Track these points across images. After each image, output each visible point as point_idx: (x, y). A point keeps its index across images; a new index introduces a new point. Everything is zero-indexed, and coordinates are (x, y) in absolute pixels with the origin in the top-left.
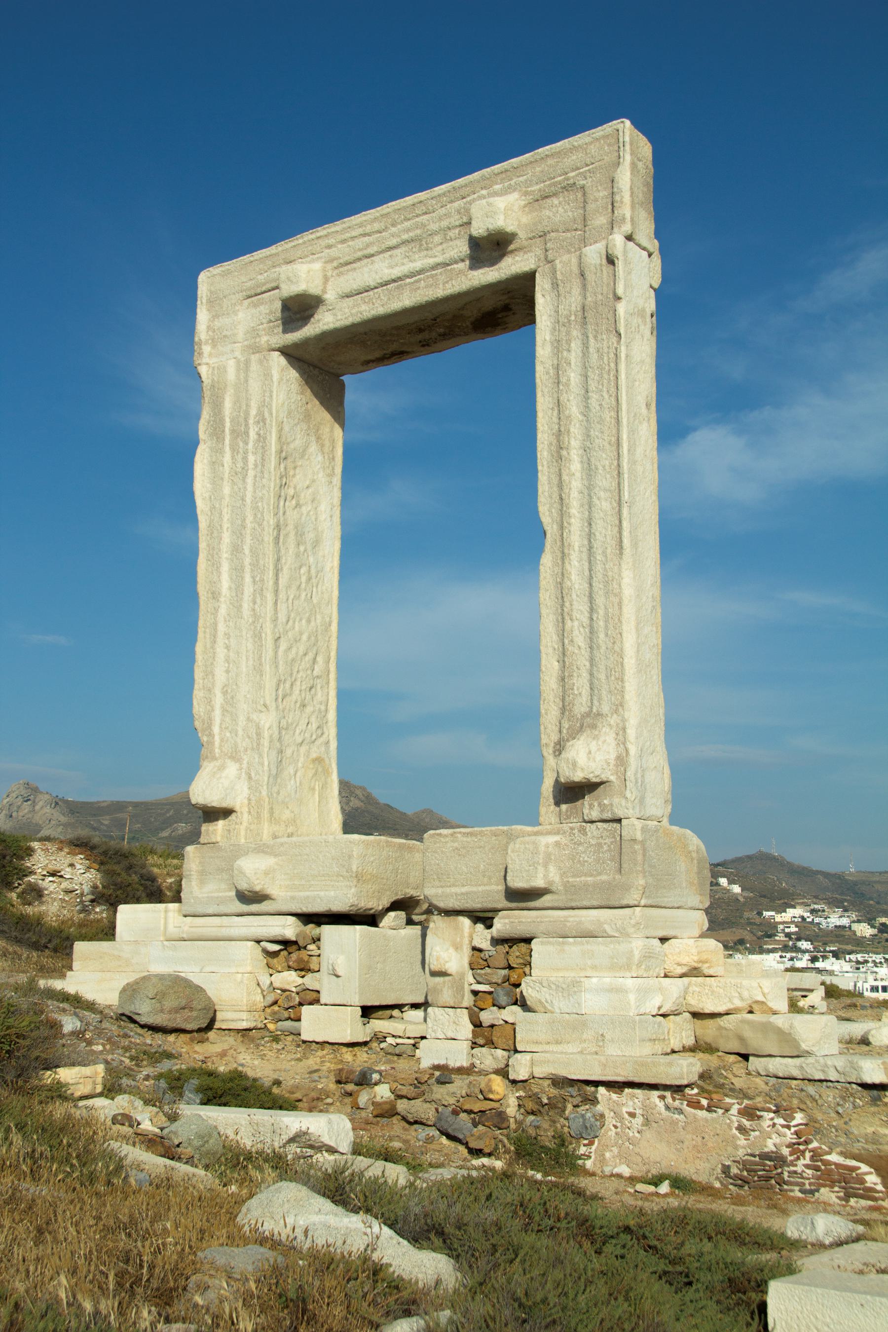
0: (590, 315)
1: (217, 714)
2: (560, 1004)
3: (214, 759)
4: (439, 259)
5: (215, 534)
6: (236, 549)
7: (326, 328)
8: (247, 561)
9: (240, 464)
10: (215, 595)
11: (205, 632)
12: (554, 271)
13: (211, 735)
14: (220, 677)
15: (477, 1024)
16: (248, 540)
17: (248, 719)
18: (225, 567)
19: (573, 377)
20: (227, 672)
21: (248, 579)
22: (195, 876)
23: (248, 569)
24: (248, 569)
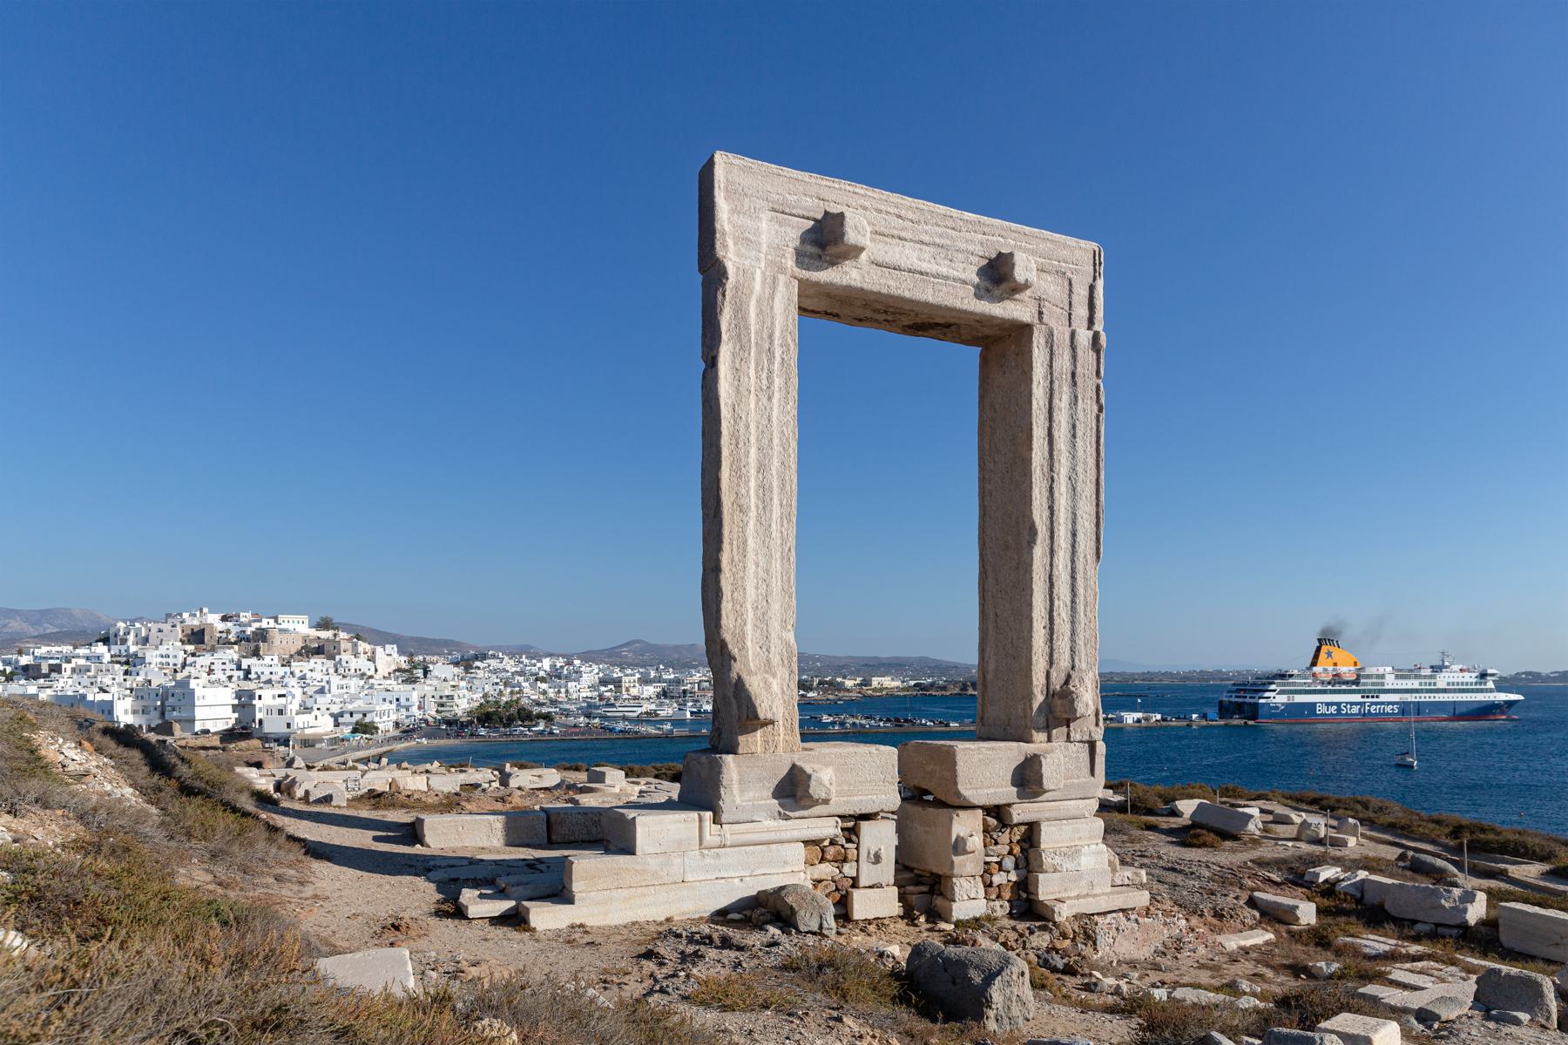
0: (1079, 380)
1: (749, 628)
2: (1068, 865)
3: (750, 673)
4: (963, 276)
5: (741, 445)
6: (762, 468)
7: (853, 283)
8: (775, 484)
9: (765, 382)
10: (743, 510)
11: (731, 544)
12: (1051, 334)
13: (743, 648)
14: (751, 592)
15: (988, 885)
16: (776, 462)
17: (780, 638)
18: (752, 484)
19: (1062, 418)
20: (757, 588)
21: (776, 501)
22: (736, 786)
23: (776, 490)
24: (776, 490)
